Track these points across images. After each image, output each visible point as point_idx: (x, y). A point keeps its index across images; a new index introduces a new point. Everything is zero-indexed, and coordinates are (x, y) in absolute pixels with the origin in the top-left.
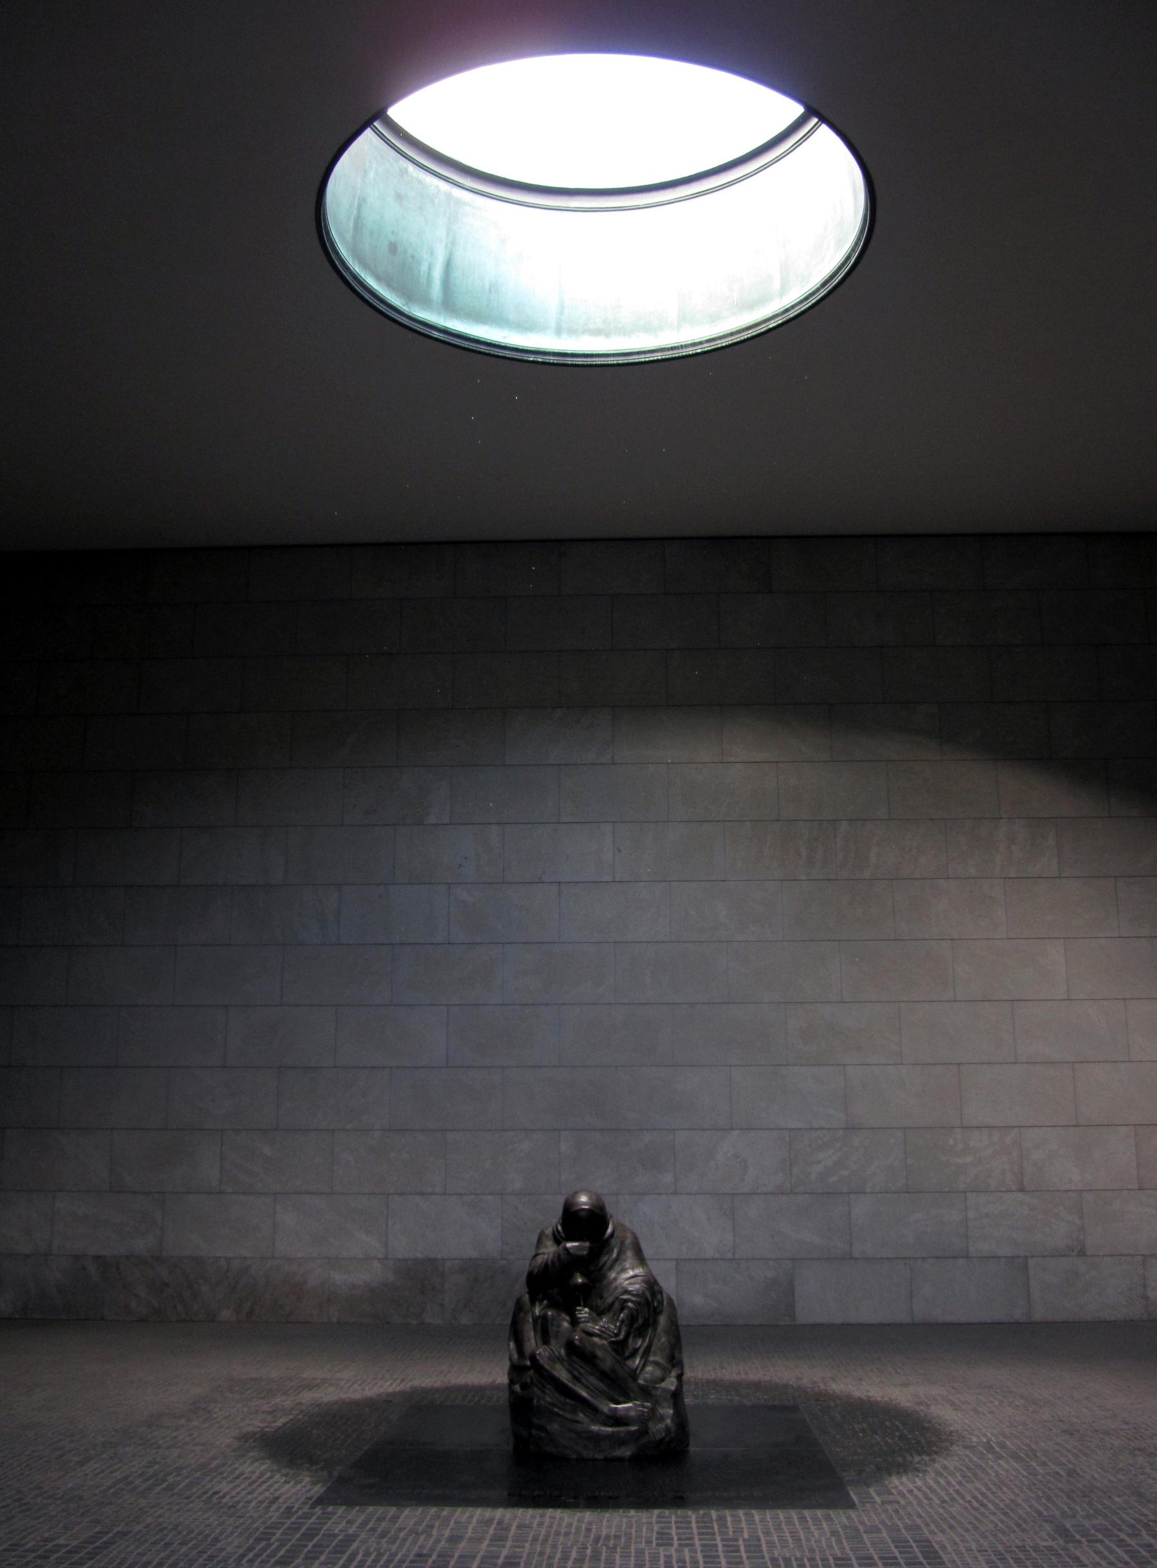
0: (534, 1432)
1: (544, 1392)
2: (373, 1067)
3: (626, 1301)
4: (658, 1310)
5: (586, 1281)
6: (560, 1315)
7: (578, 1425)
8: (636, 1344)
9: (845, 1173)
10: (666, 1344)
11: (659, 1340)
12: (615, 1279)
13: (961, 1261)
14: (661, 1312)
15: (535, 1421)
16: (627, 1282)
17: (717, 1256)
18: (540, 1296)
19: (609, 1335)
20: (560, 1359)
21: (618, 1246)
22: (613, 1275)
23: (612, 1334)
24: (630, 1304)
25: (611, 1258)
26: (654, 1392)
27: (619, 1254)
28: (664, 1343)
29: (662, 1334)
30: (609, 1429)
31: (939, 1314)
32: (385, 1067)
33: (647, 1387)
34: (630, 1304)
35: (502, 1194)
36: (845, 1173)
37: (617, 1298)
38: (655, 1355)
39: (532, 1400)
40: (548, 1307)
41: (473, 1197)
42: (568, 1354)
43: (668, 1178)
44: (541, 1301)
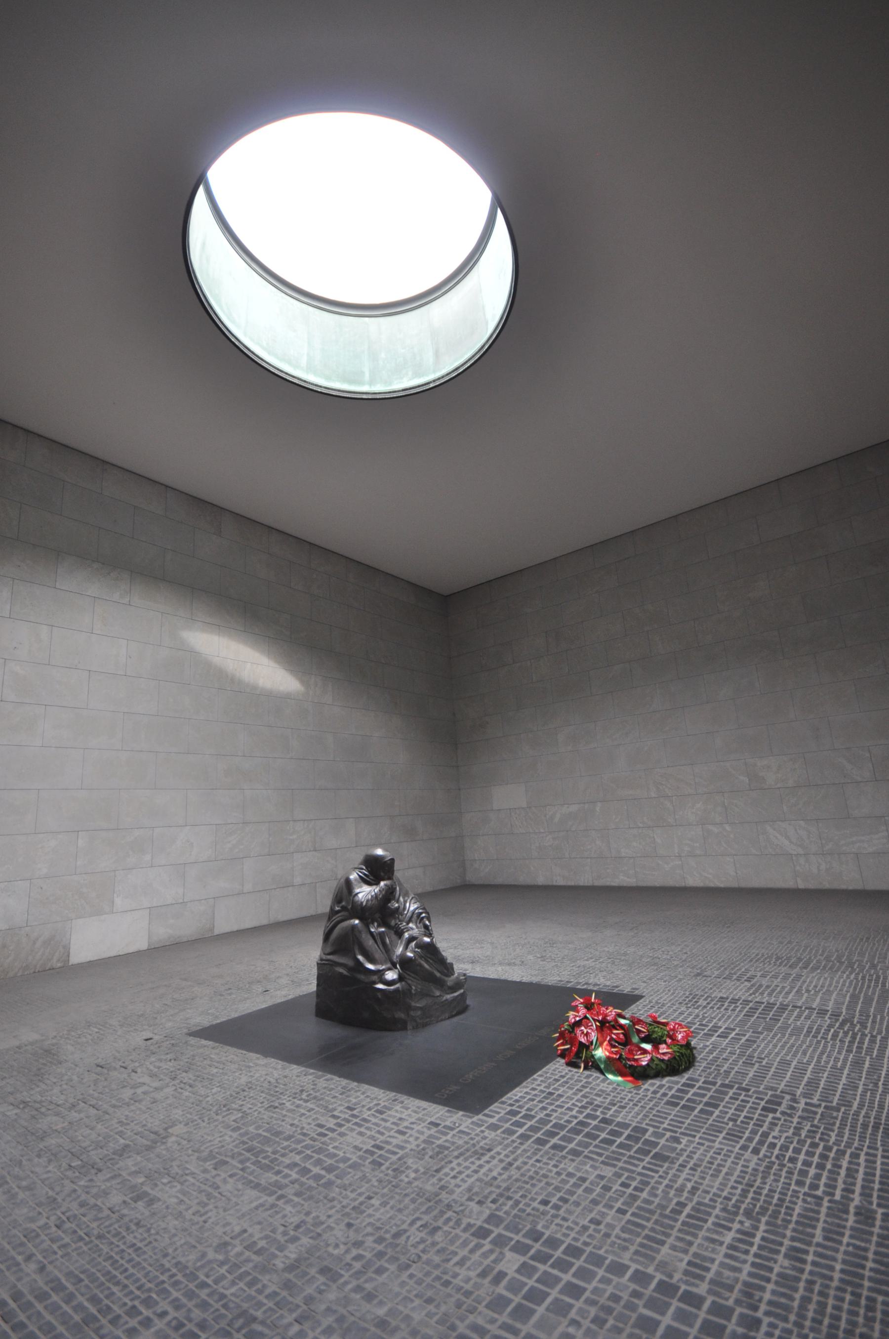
3: (421, 913)
9: (242, 847)
12: (405, 902)
13: (290, 889)
15: (413, 1004)
17: (174, 902)
20: (421, 957)
22: (401, 899)
30: (456, 994)
31: (282, 917)
34: (424, 915)
36: (242, 847)
37: (413, 913)
39: (410, 990)
43: (148, 857)
44: (373, 923)
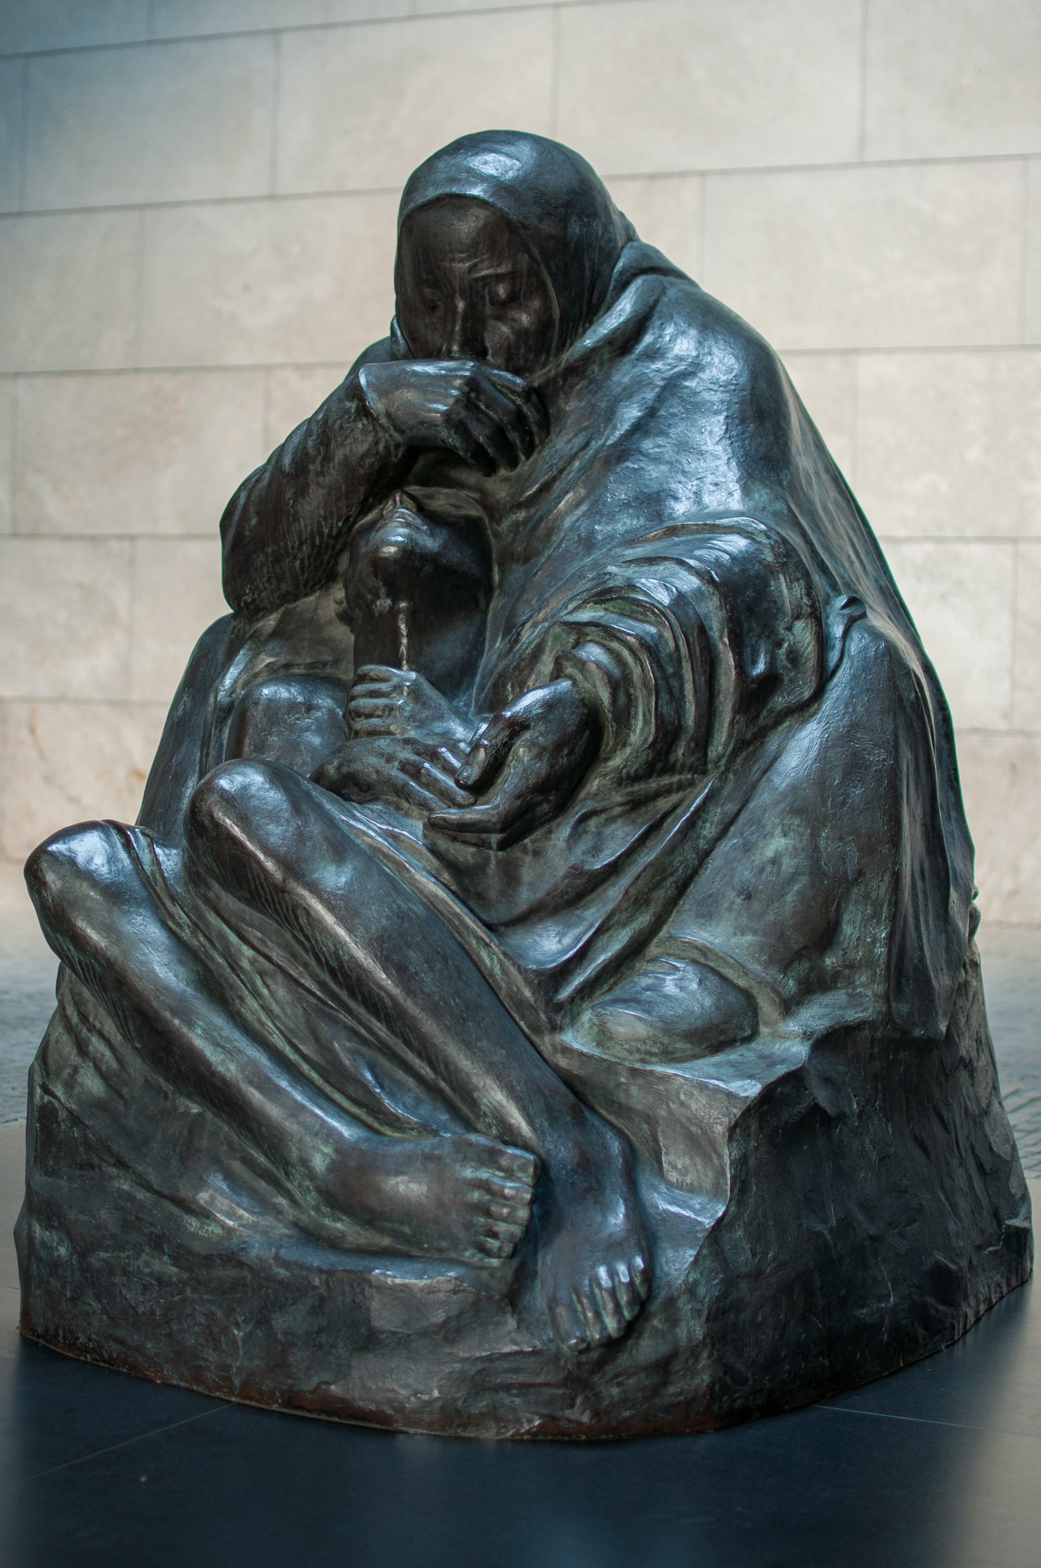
0: (37, 1229)
1: (82, 1048)
2: (653, 177)
4: (780, 701)
5: (430, 543)
6: (310, 708)
7: (193, 1223)
8: (596, 850)
10: (788, 865)
11: (748, 848)
14: (804, 709)
16: (630, 553)
18: (271, 622)
19: (445, 795)
21: (650, 395)
23: (461, 795)
24: (593, 652)
25: (594, 445)
26: (637, 1096)
27: (640, 428)
28: (775, 861)
29: (771, 820)
32: (683, 175)
33: (610, 1068)
35: (1014, 541)
38: (707, 913)
40: (279, 673)
41: (929, 547)
42: (193, 874)
44: (259, 642)
